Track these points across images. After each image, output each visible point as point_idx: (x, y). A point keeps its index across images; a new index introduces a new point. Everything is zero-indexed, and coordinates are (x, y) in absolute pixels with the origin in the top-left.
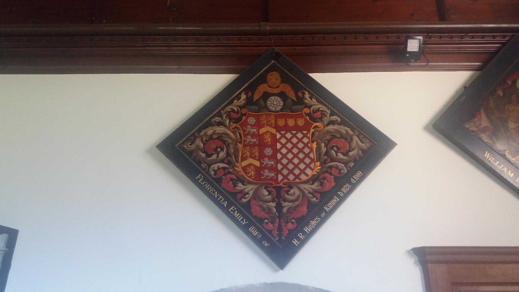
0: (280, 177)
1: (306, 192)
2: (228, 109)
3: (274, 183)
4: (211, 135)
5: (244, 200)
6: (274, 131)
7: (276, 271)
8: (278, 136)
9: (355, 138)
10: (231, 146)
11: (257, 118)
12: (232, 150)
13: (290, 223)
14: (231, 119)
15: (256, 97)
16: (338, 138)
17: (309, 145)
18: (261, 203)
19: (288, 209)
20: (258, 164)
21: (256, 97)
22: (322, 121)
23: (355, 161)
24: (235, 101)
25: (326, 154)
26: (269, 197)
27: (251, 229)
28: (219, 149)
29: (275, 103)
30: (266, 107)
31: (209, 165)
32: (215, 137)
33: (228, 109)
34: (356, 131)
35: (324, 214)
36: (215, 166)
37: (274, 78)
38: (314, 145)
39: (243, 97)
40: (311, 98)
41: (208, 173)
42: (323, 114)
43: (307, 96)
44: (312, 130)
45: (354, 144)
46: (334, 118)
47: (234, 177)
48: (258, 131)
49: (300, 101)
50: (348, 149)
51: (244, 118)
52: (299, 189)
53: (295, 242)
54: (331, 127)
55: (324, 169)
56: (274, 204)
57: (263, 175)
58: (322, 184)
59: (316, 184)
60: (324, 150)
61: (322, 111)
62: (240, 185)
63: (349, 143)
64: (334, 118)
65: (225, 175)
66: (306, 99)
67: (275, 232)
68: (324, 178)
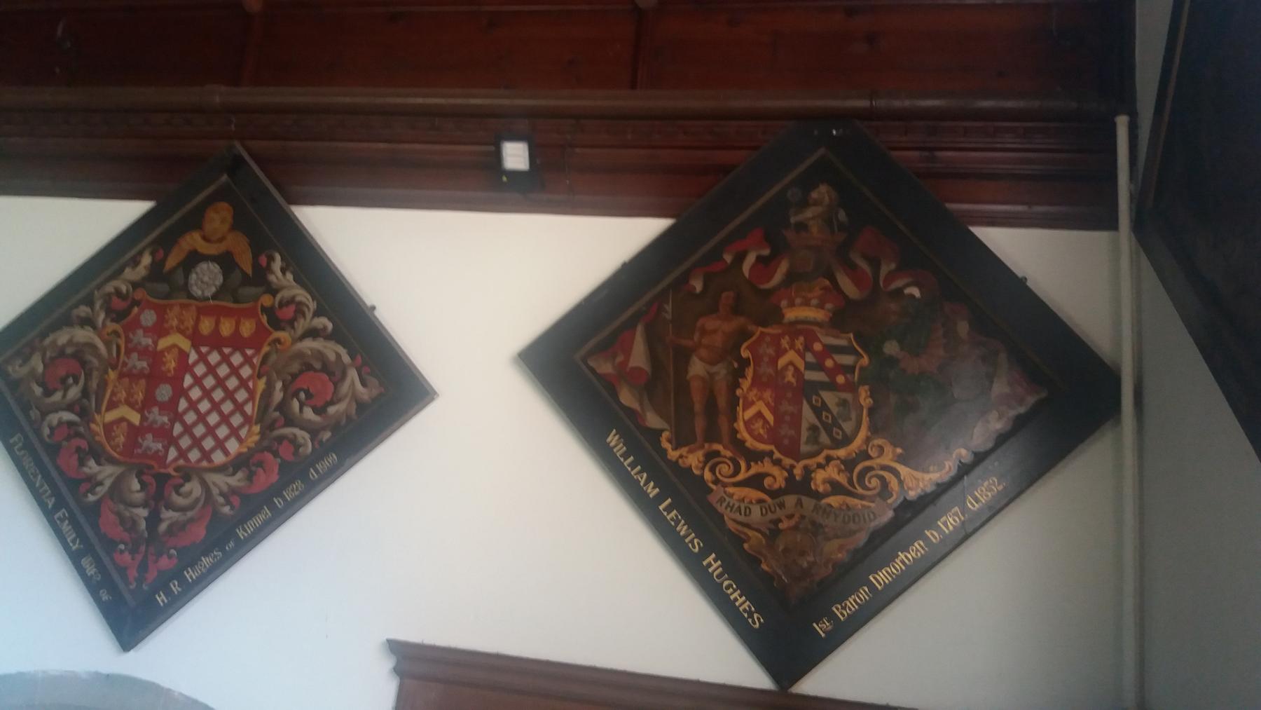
0: (173, 453)
1: (215, 491)
2: (109, 288)
3: (156, 466)
4: (64, 346)
5: (91, 498)
6: (185, 344)
8: (193, 357)
9: (353, 374)
10: (95, 374)
11: (161, 312)
12: (94, 384)
13: (165, 556)
14: (109, 311)
15: (171, 262)
16: (315, 371)
17: (251, 384)
18: (122, 507)
19: (171, 526)
20: (135, 418)
21: (171, 262)
22: (293, 328)
23: (336, 427)
24: (127, 270)
25: (283, 407)
26: (139, 497)
27: (85, 562)
28: (71, 381)
29: (206, 278)
30: (185, 289)
31: (44, 414)
32: (69, 351)
33: (109, 288)
34: (359, 357)
35: (232, 544)
37: (219, 218)
38: (262, 384)
40: (283, 271)
41: (38, 432)
42: (300, 310)
43: (277, 264)
44: (266, 349)
45: (345, 388)
46: (324, 322)
47: (83, 444)
48: (156, 343)
49: (260, 277)
50: (328, 399)
51: (136, 310)
52: (204, 484)
53: (161, 599)
54: (309, 345)
55: (266, 443)
56: (143, 512)
57: (141, 446)
58: (250, 477)
59: (240, 475)
60: (278, 396)
61: (300, 303)
62: (92, 463)
63: (335, 385)
64: (324, 322)
65: (69, 438)
66: (273, 273)
67: (133, 573)
68: (260, 464)
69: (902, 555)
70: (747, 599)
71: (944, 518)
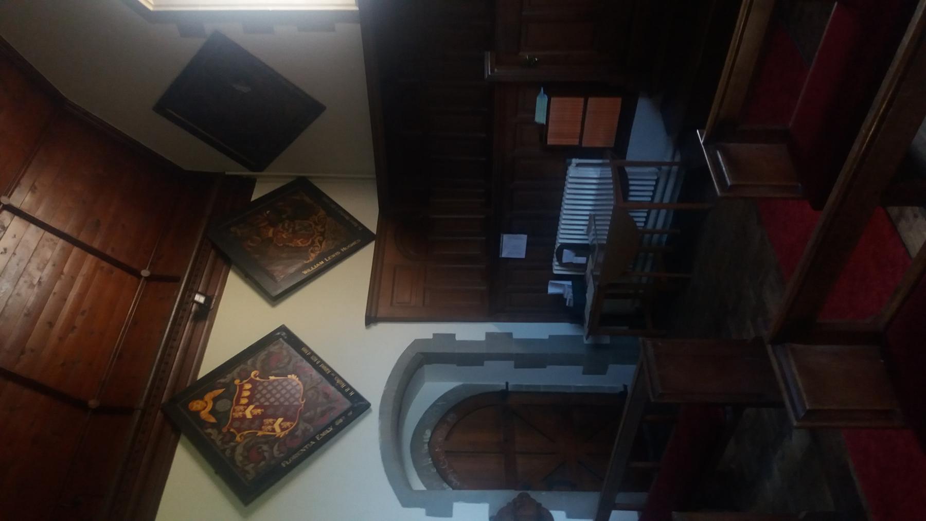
7: (371, 411)
8: (257, 404)
33: (219, 443)
36: (276, 452)
37: (196, 405)
38: (272, 378)
39: (209, 430)
43: (222, 380)
44: (258, 379)
51: (232, 430)
53: (352, 394)
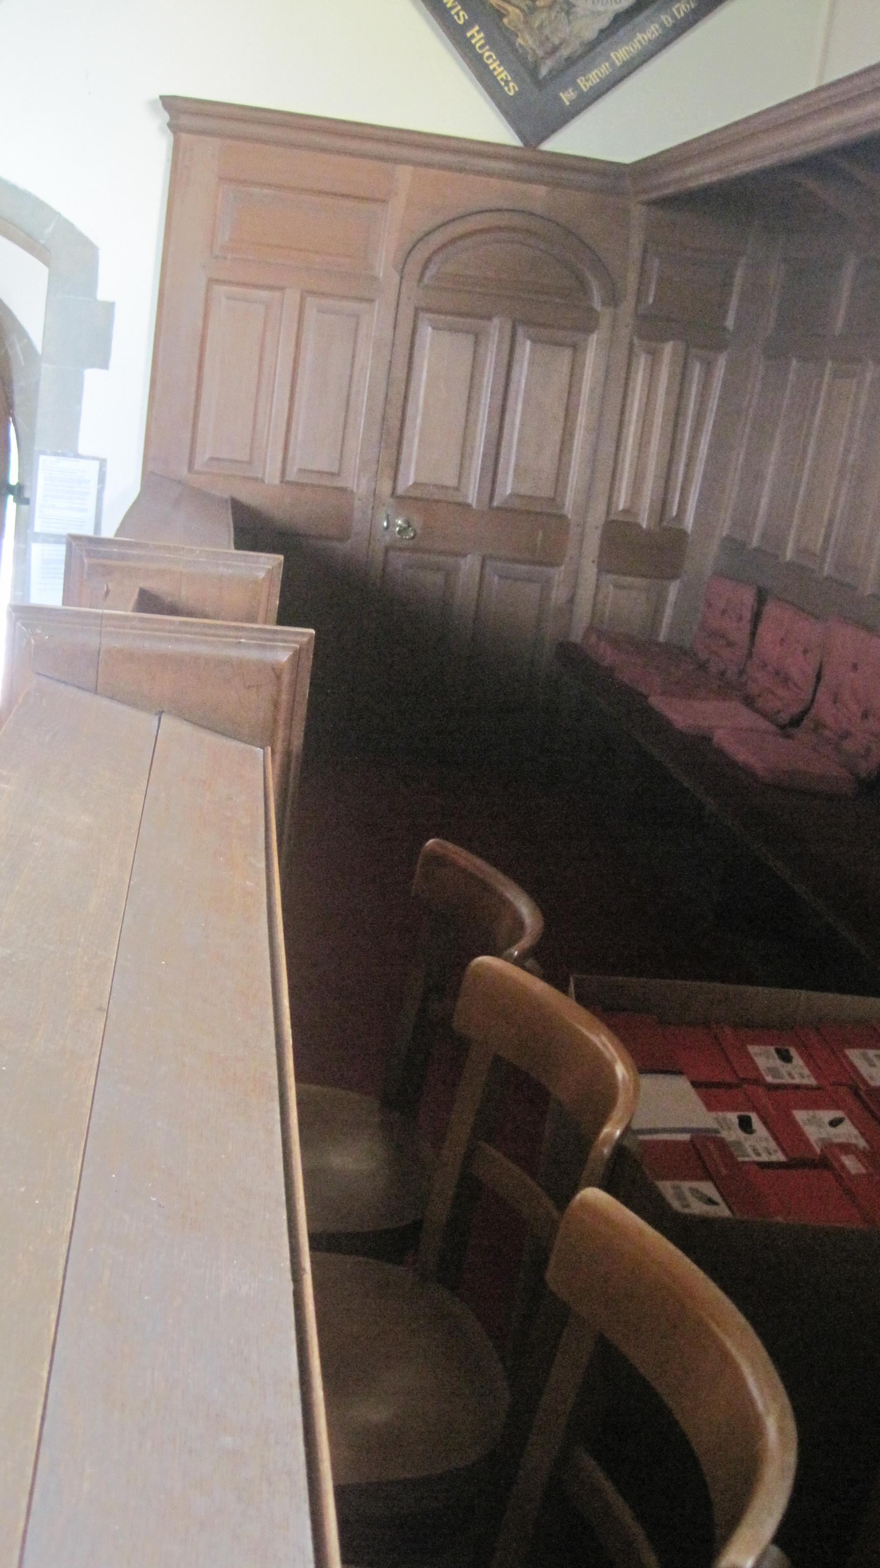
69: (639, 36)
70: (505, 69)
71: (677, 5)
